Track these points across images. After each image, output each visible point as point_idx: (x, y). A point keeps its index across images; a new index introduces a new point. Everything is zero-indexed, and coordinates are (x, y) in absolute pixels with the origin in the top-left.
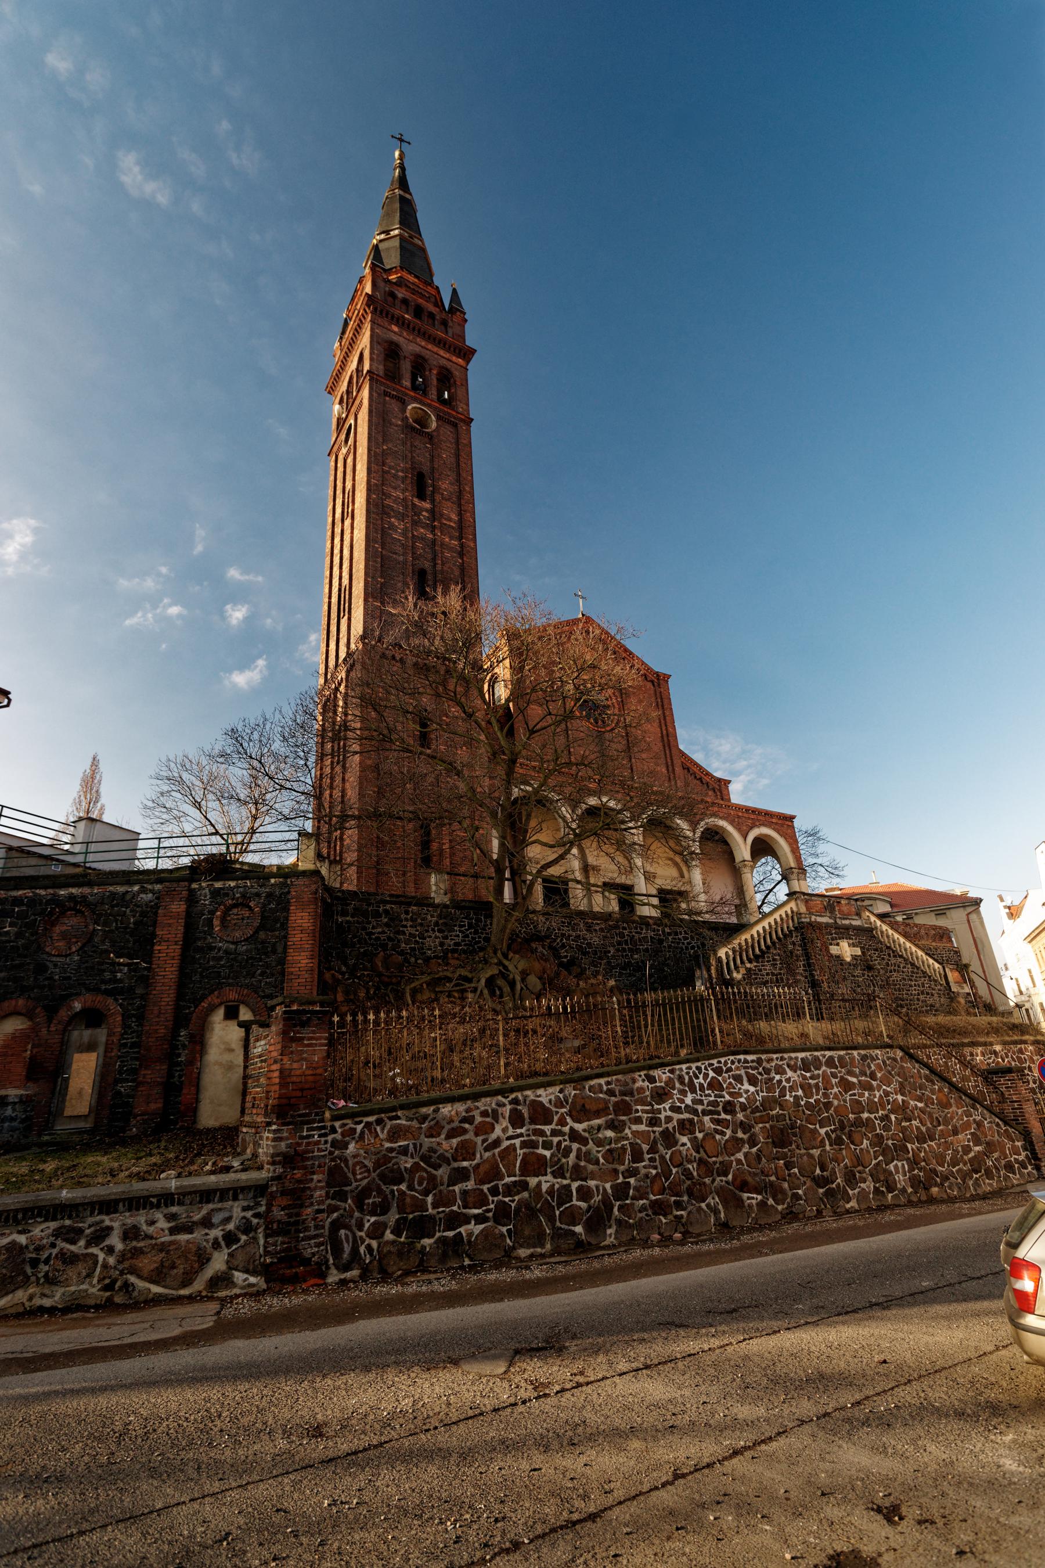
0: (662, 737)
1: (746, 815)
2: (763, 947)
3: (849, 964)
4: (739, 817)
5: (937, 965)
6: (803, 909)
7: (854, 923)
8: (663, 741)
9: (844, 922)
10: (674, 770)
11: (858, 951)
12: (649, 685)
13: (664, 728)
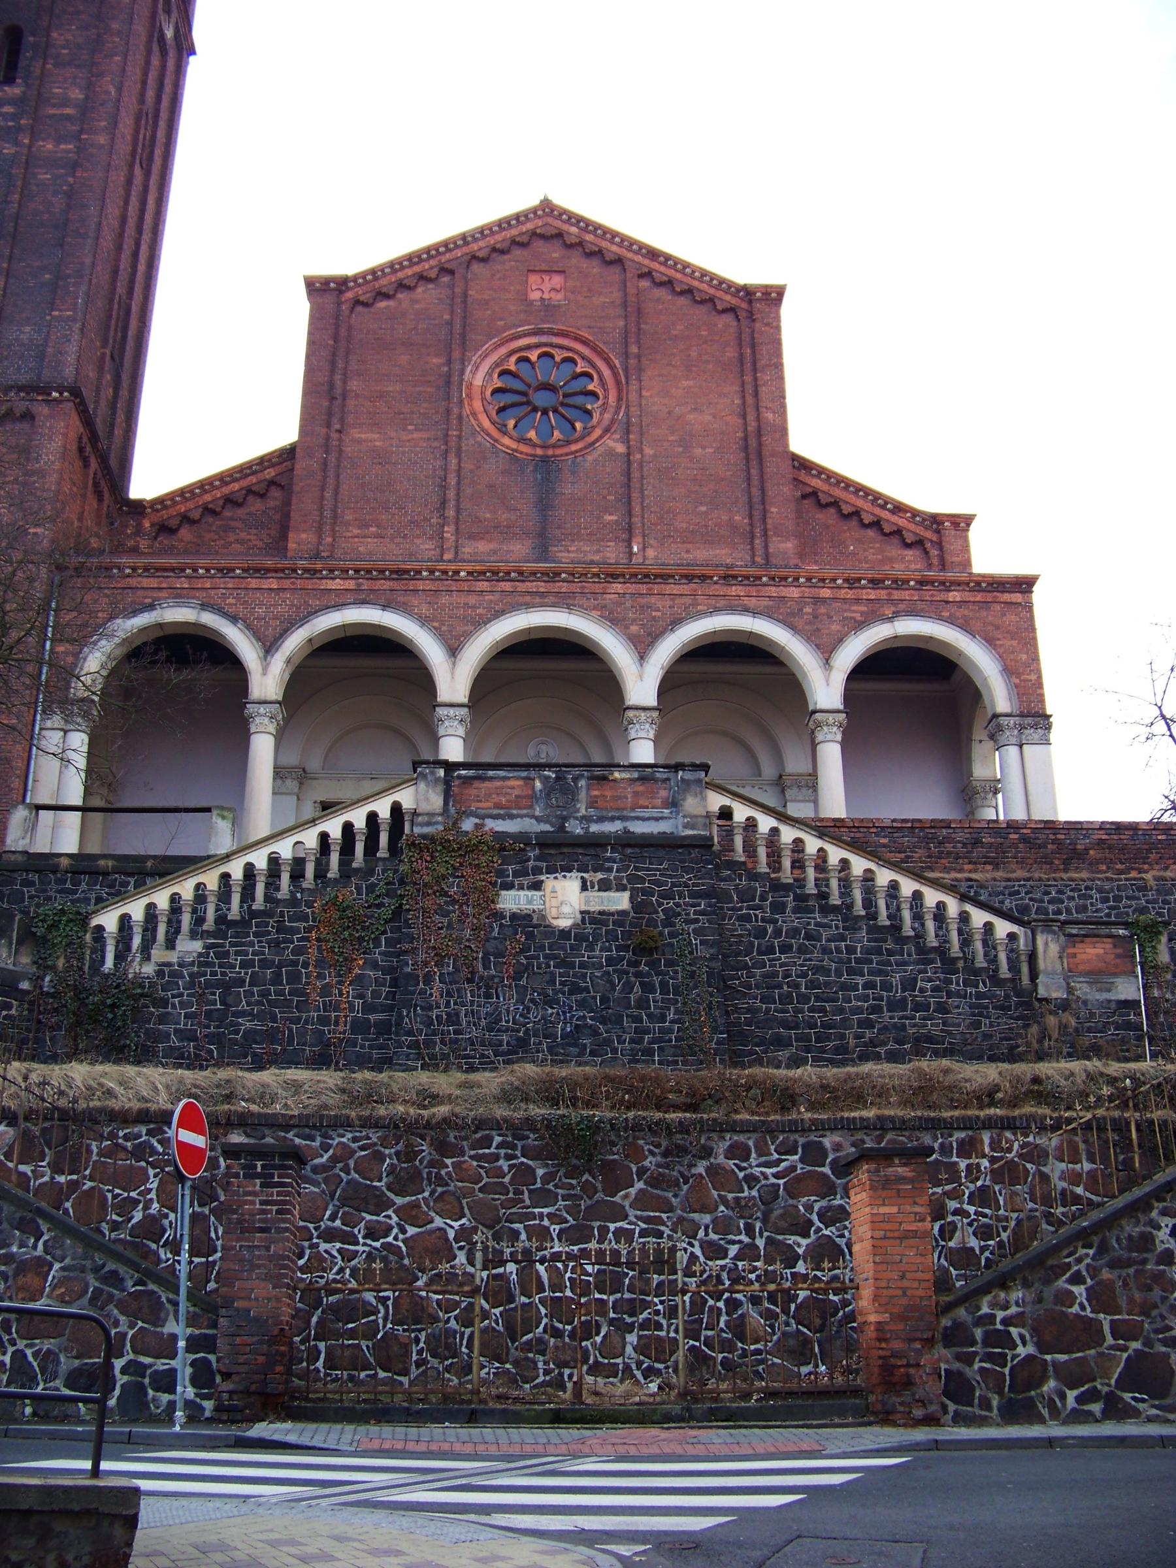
0: (745, 439)
1: (850, 594)
2: (259, 903)
3: (564, 934)
4: (818, 600)
5: (1003, 928)
6: (434, 800)
7: (639, 828)
8: (746, 448)
9: (594, 828)
10: (765, 513)
11: (621, 901)
12: (728, 319)
13: (751, 417)
